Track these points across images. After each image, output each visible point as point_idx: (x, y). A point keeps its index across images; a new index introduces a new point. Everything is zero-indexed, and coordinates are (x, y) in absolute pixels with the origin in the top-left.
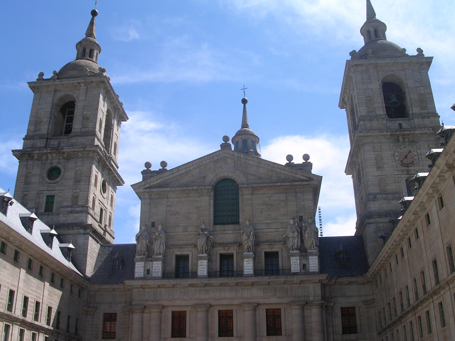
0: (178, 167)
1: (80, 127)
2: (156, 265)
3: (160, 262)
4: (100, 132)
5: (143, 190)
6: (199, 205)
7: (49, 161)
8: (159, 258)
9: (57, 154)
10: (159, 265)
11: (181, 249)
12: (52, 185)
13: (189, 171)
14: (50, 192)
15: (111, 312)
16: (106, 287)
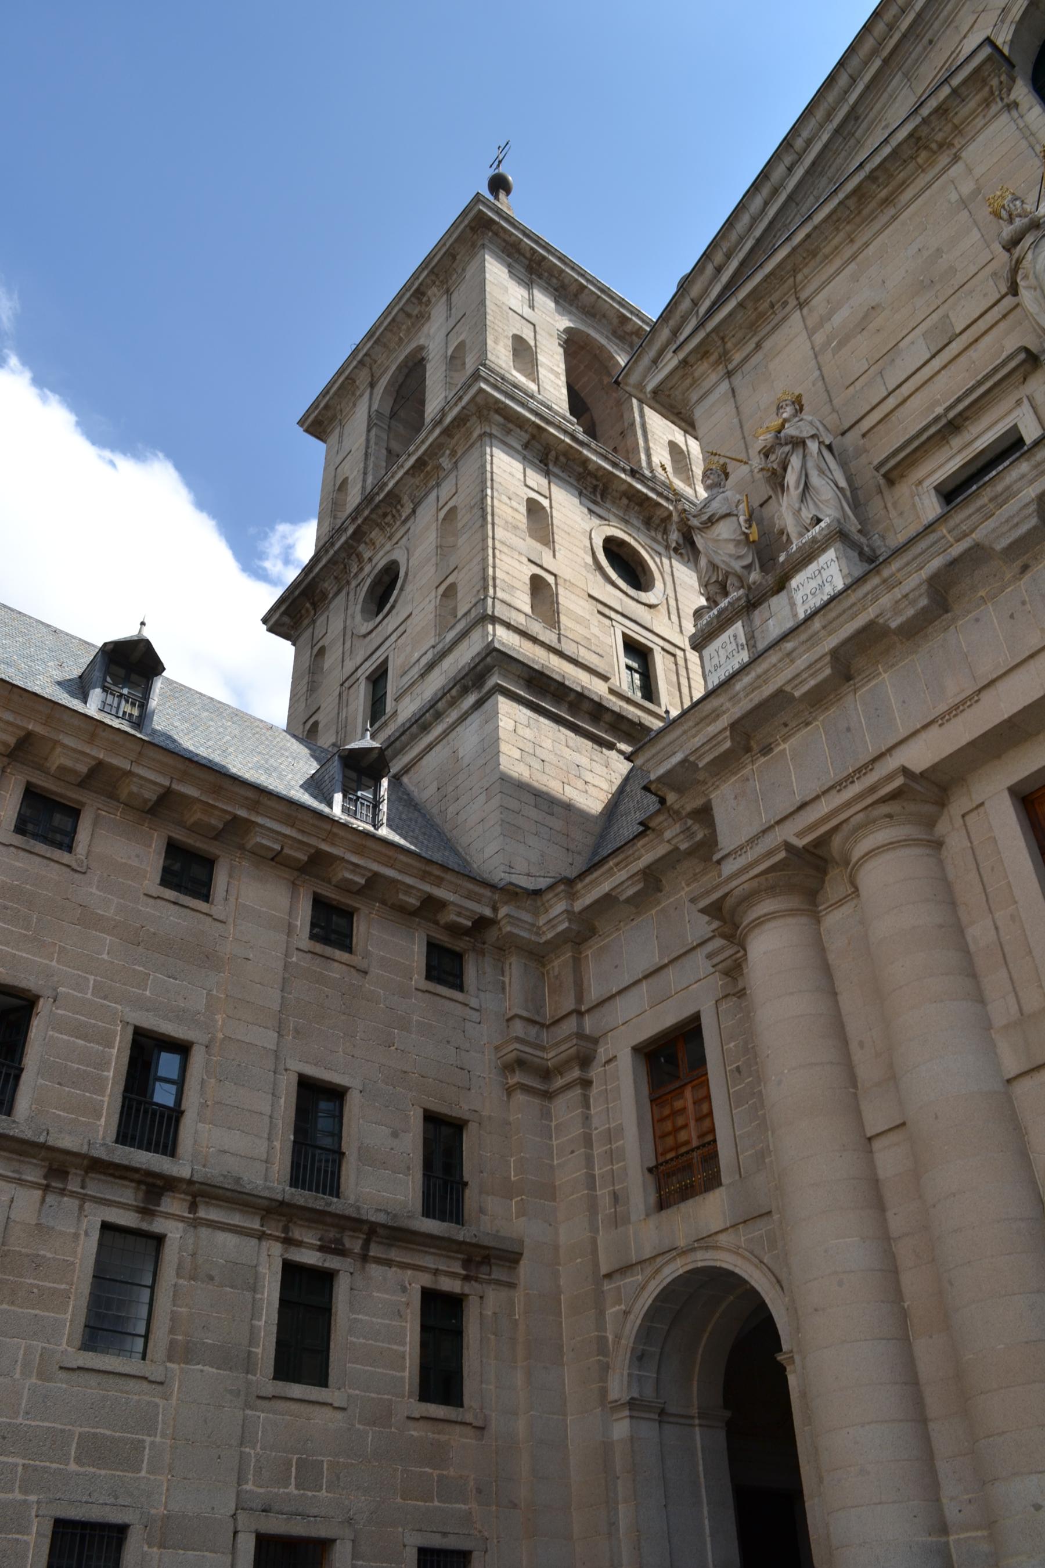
0: (787, 143)
1: (443, 395)
2: (813, 584)
3: (831, 554)
4: (534, 377)
5: (675, 362)
6: (966, 188)
7: (367, 569)
8: (814, 540)
9: (382, 529)
10: (825, 574)
11: (956, 442)
12: (380, 628)
13: (853, 116)
14: (375, 656)
15: (669, 1017)
16: (606, 887)
